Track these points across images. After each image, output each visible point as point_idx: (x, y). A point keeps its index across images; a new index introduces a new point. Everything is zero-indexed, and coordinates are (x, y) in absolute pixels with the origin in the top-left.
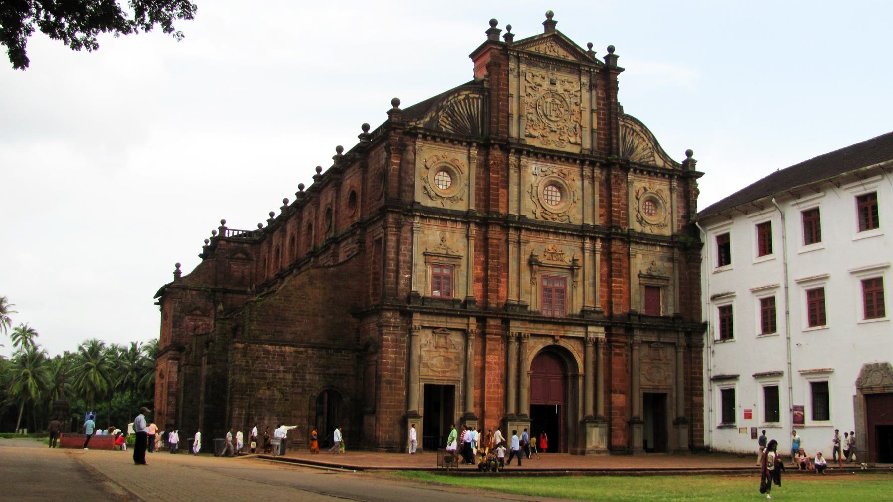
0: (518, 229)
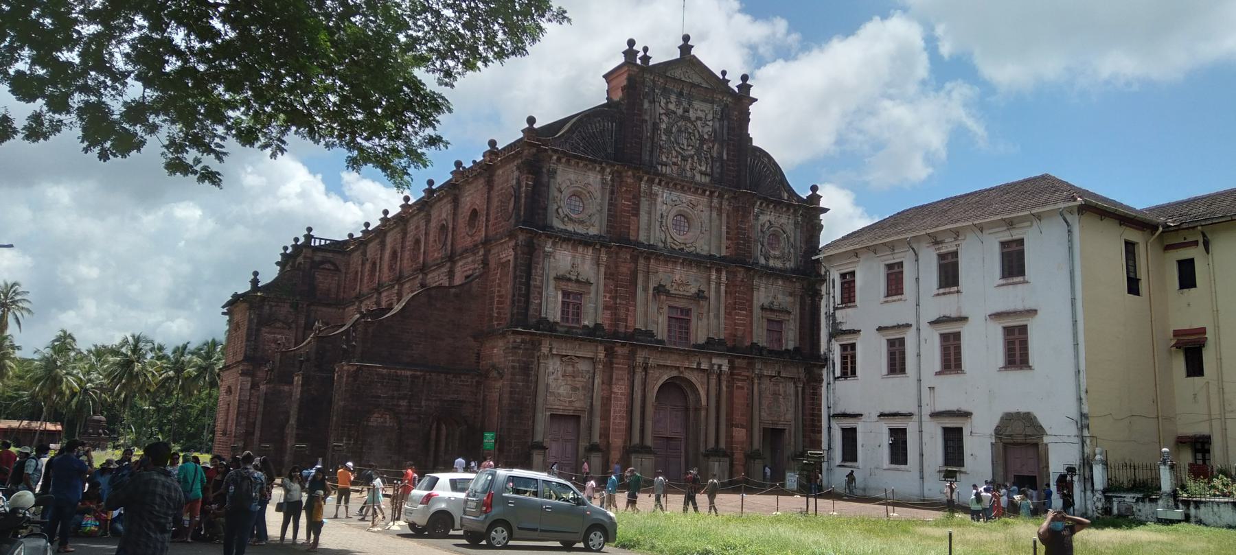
0: (648, 259)
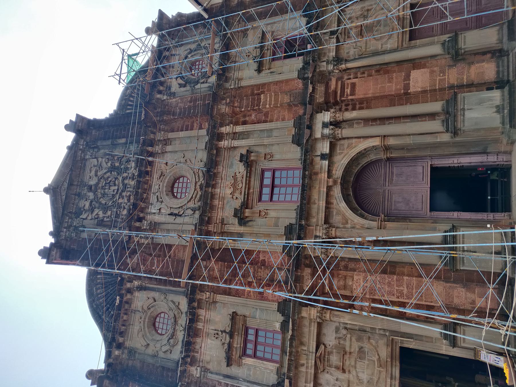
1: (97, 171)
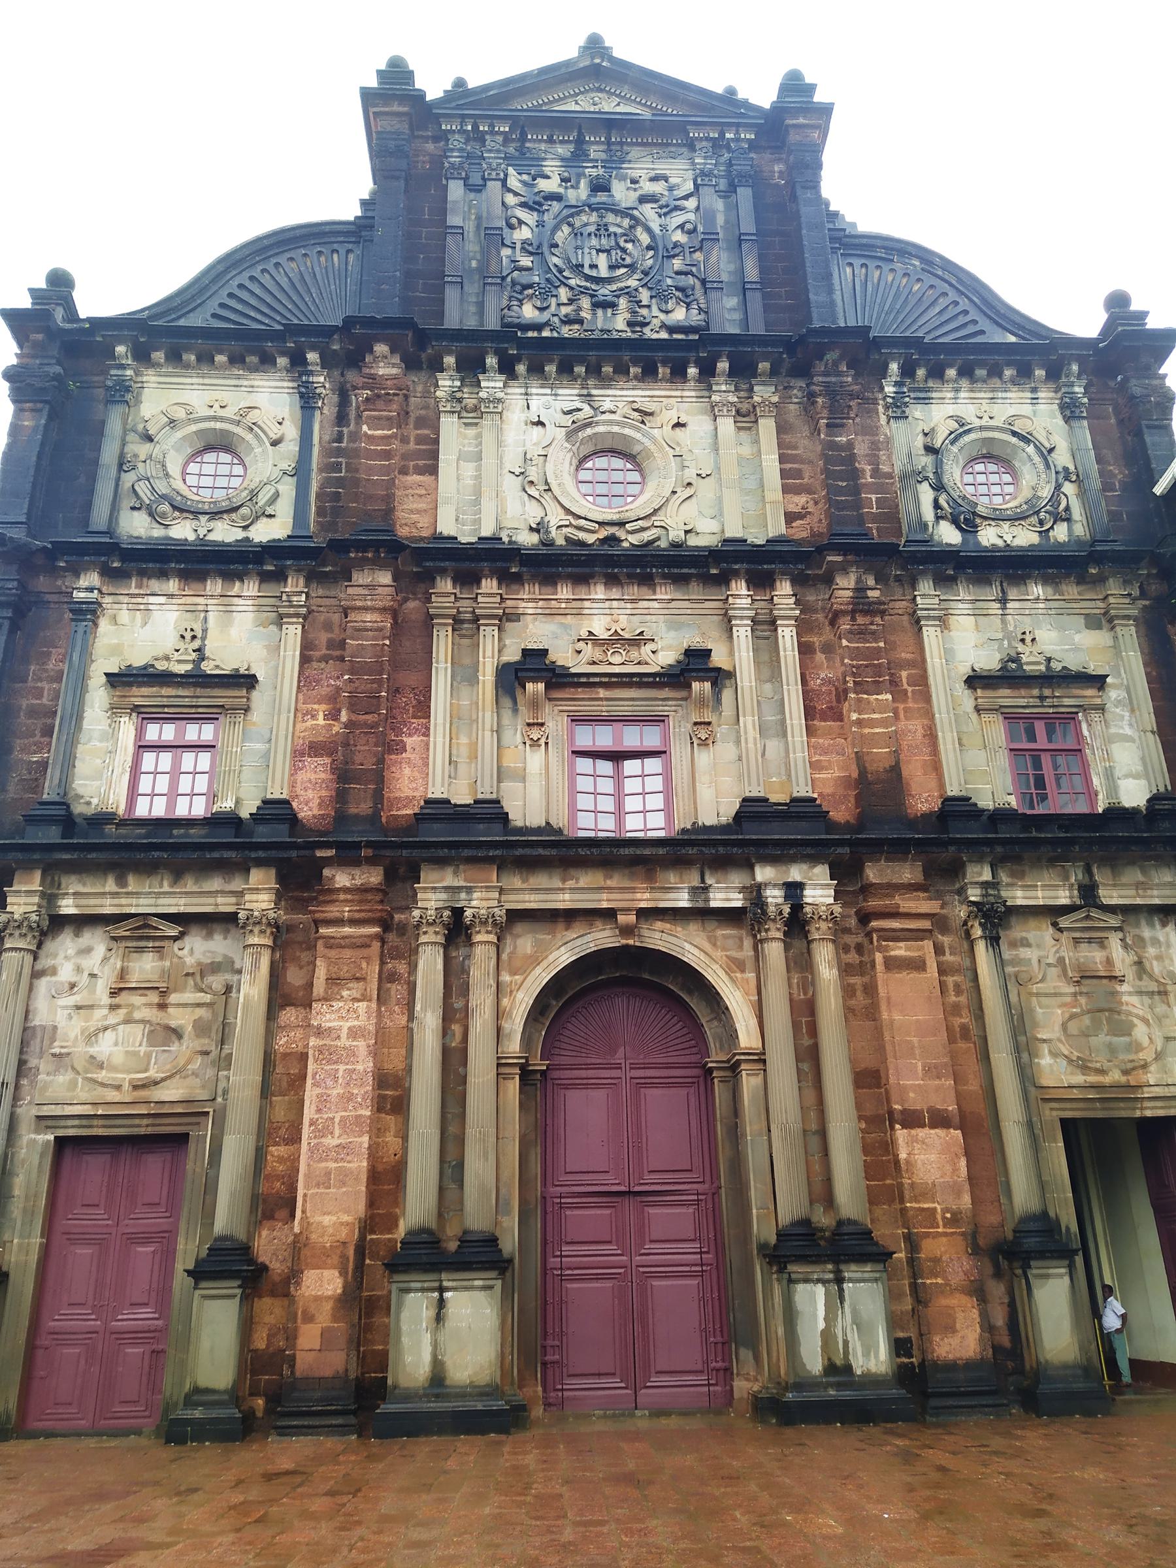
0: (468, 579)
1: (656, 201)
